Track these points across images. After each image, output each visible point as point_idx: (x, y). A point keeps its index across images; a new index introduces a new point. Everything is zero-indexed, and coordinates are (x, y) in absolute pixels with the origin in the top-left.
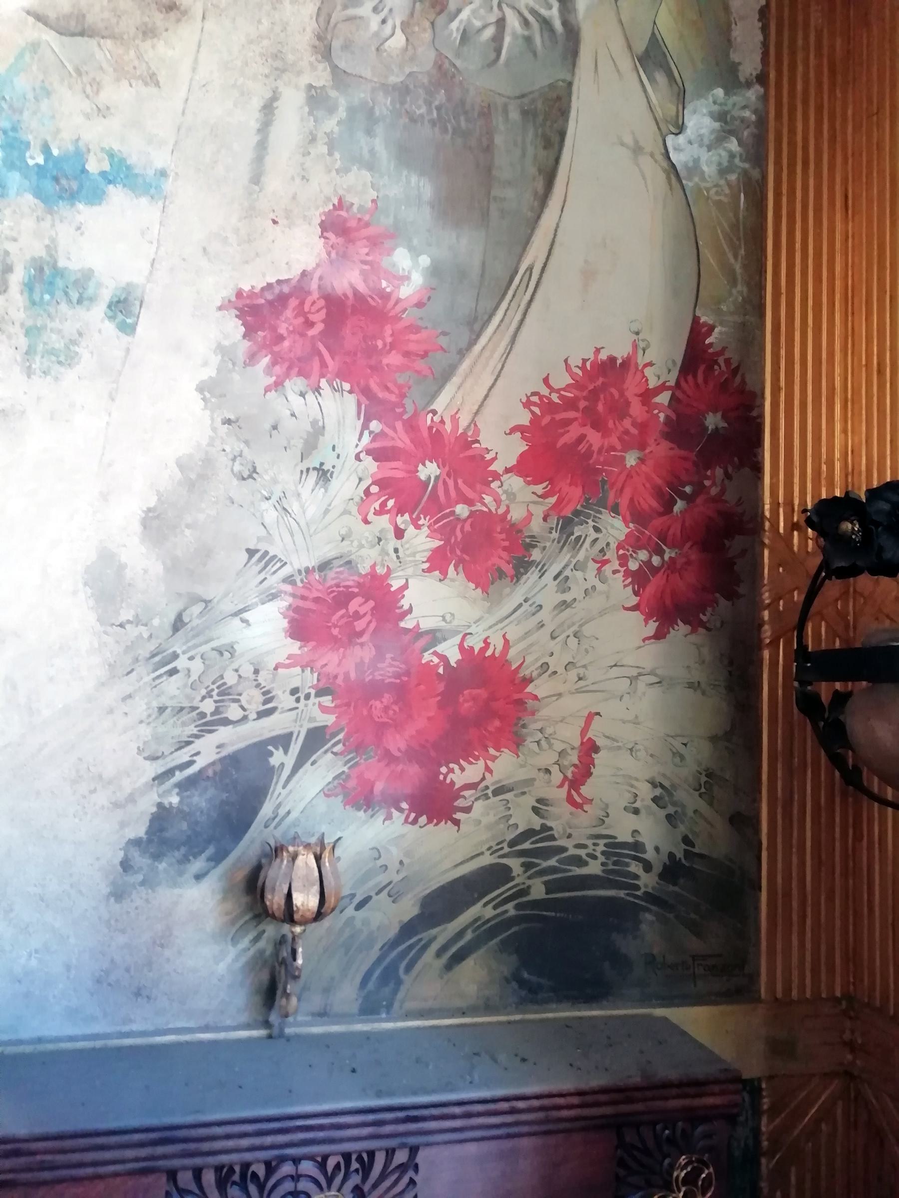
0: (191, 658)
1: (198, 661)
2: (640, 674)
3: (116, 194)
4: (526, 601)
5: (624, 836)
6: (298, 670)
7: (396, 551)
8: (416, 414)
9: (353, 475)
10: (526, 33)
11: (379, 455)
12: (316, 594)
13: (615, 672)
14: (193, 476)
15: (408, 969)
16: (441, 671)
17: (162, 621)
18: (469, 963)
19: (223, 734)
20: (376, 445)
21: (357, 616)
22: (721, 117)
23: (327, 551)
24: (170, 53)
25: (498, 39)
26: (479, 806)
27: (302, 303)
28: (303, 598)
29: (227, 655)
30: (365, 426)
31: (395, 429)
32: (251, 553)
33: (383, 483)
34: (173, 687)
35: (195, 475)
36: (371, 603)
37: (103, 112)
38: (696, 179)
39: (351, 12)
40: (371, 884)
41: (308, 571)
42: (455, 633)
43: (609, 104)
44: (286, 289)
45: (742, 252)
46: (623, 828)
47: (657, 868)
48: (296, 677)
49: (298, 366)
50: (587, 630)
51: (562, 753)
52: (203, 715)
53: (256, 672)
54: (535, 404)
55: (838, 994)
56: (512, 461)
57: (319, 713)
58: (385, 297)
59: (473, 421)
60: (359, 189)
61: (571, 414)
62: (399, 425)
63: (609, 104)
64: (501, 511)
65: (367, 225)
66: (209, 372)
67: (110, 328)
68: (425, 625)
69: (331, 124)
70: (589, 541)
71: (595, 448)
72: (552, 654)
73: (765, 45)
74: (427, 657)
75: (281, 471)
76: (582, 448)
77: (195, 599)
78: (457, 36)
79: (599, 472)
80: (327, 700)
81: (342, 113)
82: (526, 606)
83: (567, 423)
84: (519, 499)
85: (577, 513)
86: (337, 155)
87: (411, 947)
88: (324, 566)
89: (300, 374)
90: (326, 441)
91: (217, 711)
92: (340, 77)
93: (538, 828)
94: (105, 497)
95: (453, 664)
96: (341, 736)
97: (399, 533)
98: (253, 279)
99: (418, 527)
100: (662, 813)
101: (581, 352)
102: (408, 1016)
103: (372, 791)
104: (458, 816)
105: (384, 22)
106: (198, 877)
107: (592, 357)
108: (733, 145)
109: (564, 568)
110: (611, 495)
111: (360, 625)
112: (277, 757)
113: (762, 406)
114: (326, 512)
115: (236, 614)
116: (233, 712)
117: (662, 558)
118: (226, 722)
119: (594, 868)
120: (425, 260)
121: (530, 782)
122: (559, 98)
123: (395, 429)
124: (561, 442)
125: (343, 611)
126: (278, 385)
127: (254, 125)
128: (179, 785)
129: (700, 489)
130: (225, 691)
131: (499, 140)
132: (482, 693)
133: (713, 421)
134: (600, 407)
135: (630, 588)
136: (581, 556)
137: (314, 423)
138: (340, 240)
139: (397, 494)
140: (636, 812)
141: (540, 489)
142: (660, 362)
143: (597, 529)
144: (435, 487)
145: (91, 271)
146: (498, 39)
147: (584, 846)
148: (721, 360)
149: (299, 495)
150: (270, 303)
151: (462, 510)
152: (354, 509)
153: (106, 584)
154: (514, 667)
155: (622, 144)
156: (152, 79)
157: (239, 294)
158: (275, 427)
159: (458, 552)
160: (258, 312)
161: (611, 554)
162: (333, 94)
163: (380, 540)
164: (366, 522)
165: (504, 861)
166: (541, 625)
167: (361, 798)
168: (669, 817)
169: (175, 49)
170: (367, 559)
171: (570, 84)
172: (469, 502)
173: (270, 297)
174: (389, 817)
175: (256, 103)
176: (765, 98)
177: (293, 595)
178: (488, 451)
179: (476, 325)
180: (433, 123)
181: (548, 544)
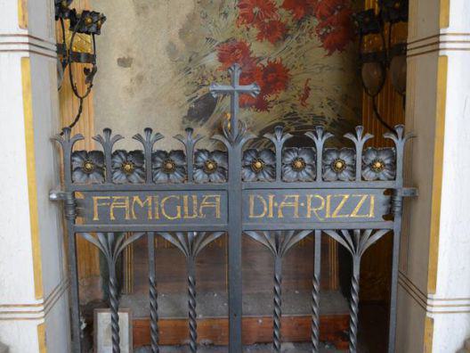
5: (318, 114)
11: (241, 7)
19: (204, 88)
23: (228, 37)
34: (190, 76)
35: (191, 18)
46: (318, 112)
47: (329, 123)
48: (221, 73)
56: (282, 4)
68: (257, 56)
77: (194, 53)
88: (227, 41)
94: (169, 27)
97: (248, 29)
100: (330, 109)
106: (201, 125)
116: (206, 83)
121: (290, 99)
132: (274, 74)
139: (248, 18)
141: (290, 12)
151: (266, 21)
153: (171, 50)
161: (314, 30)
166: (292, 53)
170: (240, 37)
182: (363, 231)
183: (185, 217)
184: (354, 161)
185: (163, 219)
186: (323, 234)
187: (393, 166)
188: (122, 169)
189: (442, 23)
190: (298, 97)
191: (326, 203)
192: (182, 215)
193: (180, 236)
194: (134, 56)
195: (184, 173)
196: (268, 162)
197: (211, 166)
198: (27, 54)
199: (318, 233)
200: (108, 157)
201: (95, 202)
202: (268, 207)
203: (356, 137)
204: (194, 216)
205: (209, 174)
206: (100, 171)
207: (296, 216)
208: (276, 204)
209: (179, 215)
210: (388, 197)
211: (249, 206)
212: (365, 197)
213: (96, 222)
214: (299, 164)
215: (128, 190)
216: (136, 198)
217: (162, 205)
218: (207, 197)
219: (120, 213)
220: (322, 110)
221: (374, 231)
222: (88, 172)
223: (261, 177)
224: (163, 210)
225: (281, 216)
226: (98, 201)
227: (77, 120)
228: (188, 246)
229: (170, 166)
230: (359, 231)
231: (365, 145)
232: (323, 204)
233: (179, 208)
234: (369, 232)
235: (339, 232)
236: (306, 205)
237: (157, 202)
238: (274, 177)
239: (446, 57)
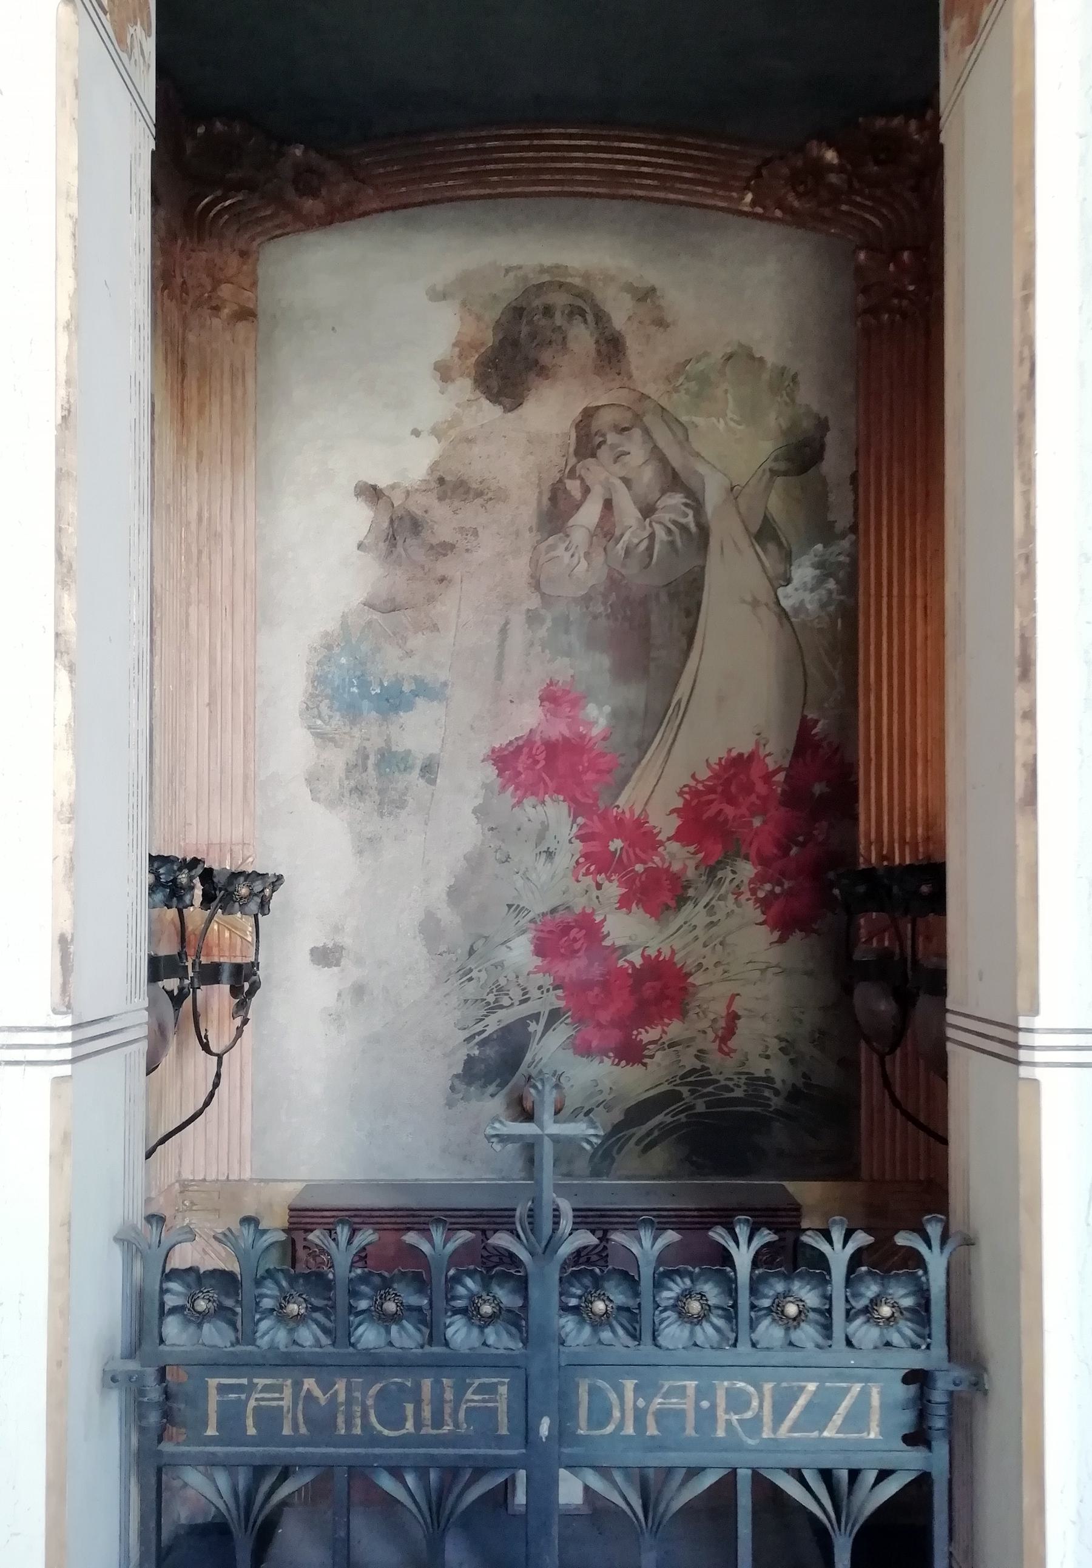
0: (480, 971)
1: (484, 972)
2: (768, 968)
3: (420, 702)
4: (685, 923)
5: (760, 1073)
7: (598, 897)
8: (606, 810)
9: (569, 852)
10: (670, 538)
11: (582, 838)
15: (619, 1151)
16: (630, 971)
17: (462, 951)
18: (657, 1149)
19: (501, 1013)
20: (582, 832)
21: (575, 940)
22: (820, 565)
24: (444, 608)
25: (650, 549)
26: (659, 1055)
27: (531, 749)
28: (542, 931)
30: (574, 821)
31: (592, 820)
32: (510, 906)
33: (586, 856)
34: (471, 989)
35: (475, 862)
36: (584, 932)
37: (409, 654)
38: (802, 616)
39: (553, 554)
40: (594, 1101)
42: (639, 947)
43: (733, 574)
44: (521, 742)
45: (840, 662)
46: (759, 1068)
49: (531, 789)
50: (729, 940)
51: (714, 1020)
52: (488, 1003)
53: (517, 977)
54: (686, 793)
55: (922, 1178)
56: (672, 833)
57: (555, 1000)
58: (582, 737)
59: (644, 810)
60: (563, 669)
61: (713, 796)
62: (595, 818)
63: (733, 574)
64: (666, 865)
65: (569, 692)
66: (480, 801)
67: (422, 782)
68: (618, 943)
69: (543, 632)
70: (728, 880)
71: (730, 817)
73: (856, 501)
74: (621, 963)
76: (721, 819)
77: (481, 936)
78: (622, 553)
80: (560, 992)
81: (549, 623)
82: (685, 927)
83: (711, 802)
84: (677, 857)
85: (719, 862)
86: (547, 651)
87: (619, 1139)
88: (553, 911)
89: (532, 794)
91: (496, 1001)
92: (547, 600)
93: (699, 1067)
94: (426, 882)
95: (638, 966)
96: (569, 1014)
97: (599, 886)
98: (501, 740)
99: (611, 881)
100: (786, 1058)
101: (717, 752)
102: (619, 1179)
103: (590, 1046)
104: (646, 1060)
105: (572, 556)
106: (492, 1096)
107: (725, 755)
108: (831, 584)
109: (711, 899)
111: (577, 946)
112: (532, 1027)
113: (857, 773)
116: (505, 1001)
118: (502, 1007)
119: (738, 1093)
120: (607, 709)
121: (692, 1039)
122: (695, 580)
123: (592, 820)
124: (705, 817)
126: (519, 803)
127: (495, 643)
128: (477, 1044)
130: (500, 989)
131: (654, 618)
133: (818, 788)
134: (733, 789)
136: (723, 891)
137: (543, 823)
138: (552, 706)
139: (597, 862)
140: (768, 1057)
141: (692, 849)
142: (776, 752)
143: (734, 872)
144: (621, 854)
145: (410, 751)
146: (650, 549)
147: (731, 1079)
148: (825, 744)
150: (512, 752)
151: (639, 868)
152: (570, 874)
153: (430, 929)
154: (679, 966)
155: (744, 601)
156: (435, 628)
157: (493, 751)
160: (505, 760)
161: (744, 888)
162: (543, 612)
164: (578, 881)
165: (677, 1088)
166: (696, 938)
167: (584, 1050)
168: (792, 1061)
169: (447, 607)
170: (580, 904)
171: (703, 568)
172: (644, 862)
173: (511, 749)
174: (602, 1062)
175: (496, 629)
176: (855, 544)
178: (655, 827)
179: (643, 746)
180: (608, 616)
182: (854, 1474)
184: (829, 1298)
185: (373, 1439)
186: (758, 1479)
187: (921, 1313)
188: (279, 1314)
189: (1022, 1003)
190: (711, 1035)
191: (761, 1400)
192: (418, 1424)
193: (410, 1479)
194: (347, 941)
195: (423, 1322)
196: (620, 1298)
198: (66, 1070)
199: (744, 1474)
200: (247, 1284)
202: (623, 1411)
203: (830, 1242)
204: (446, 1429)
205: (482, 1328)
206: (222, 1312)
207: (690, 1431)
208: (641, 1403)
210: (913, 1389)
211: (578, 1405)
212: (857, 1388)
214: (695, 1306)
215: (290, 1363)
216: (309, 1383)
217: (370, 1402)
219: (269, 1418)
220: (766, 1064)
221: (883, 1475)
222: (202, 1318)
223: (606, 1335)
224: (372, 1412)
225: (652, 1430)
226: (222, 1389)
227: (207, 1104)
228: (430, 1509)
229: (391, 1307)
230: (844, 1474)
231: (855, 1260)
232: (755, 1403)
233: (409, 1408)
234: (871, 1476)
235: (798, 1475)
236: (713, 1406)
237: (357, 1394)
238: (636, 1336)
239: (1035, 1082)
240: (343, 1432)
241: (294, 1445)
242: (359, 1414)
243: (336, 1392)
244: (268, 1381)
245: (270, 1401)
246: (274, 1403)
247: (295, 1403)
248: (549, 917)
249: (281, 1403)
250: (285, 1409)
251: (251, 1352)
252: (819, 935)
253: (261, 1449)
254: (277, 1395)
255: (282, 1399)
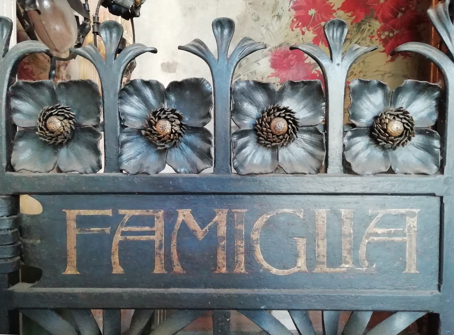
0: (244, 75)
2: (385, 73)
6: (274, 77)
7: (302, 39)
12: (278, 54)
13: (377, 73)
14: (241, 21)
16: (318, 75)
20: (295, 5)
21: (291, 60)
23: (281, 41)
28: (275, 56)
29: (254, 74)
33: (297, 17)
36: (295, 56)
41: (276, 47)
50: (367, 60)
56: (340, 6)
70: (367, 30)
72: (354, 68)
75: (267, 17)
79: (371, 6)
88: (280, 45)
90: (280, 6)
97: (303, 33)
99: (309, 30)
109: (359, 39)
110: (375, 14)
111: (292, 63)
114: (280, 29)
115: (256, 62)
117: (394, 33)
125: (286, 59)
129: (407, 8)
135: (382, 45)
136: (364, 35)
141: (349, 14)
143: (370, 26)
144: (314, 16)
149: (272, 24)
152: (289, 27)
158: (264, 4)
159: (322, 38)
161: (375, 34)
163: (297, 36)
164: (293, 30)
177: (272, 55)
178: (331, 3)
181: (353, 32)
183: (316, 270)
188: (148, 134)
197: (396, 127)
200: (110, 98)
201: (72, 224)
209: (301, 263)
213: (72, 281)
218: (381, 213)
219: (138, 255)
226: (82, 222)
229: (281, 125)
237: (241, 227)
240: (224, 270)
241: (167, 286)
242: (242, 250)
243: (216, 224)
244: (137, 213)
245: (139, 234)
246: (144, 238)
247: (168, 239)
248: (278, 49)
249: (152, 237)
250: (157, 245)
251: (115, 178)
252: (411, 57)
253: (129, 290)
254: (147, 228)
255: (153, 233)
